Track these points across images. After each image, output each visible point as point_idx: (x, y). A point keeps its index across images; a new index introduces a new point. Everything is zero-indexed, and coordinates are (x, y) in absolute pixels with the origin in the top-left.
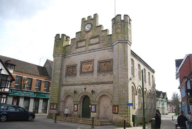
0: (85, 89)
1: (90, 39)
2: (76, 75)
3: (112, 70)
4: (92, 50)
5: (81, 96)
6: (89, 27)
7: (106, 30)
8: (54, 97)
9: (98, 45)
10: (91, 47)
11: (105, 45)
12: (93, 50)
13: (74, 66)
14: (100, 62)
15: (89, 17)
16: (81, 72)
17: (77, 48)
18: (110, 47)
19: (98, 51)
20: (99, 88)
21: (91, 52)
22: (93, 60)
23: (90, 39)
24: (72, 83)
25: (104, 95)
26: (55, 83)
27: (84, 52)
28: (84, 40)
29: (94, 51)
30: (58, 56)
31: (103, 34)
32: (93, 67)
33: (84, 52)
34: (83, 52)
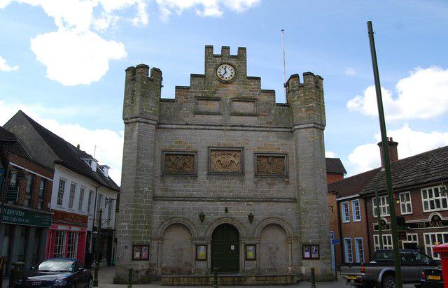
0: (226, 210)
1: (234, 100)
2: (195, 176)
3: (287, 177)
4: (241, 126)
5: (215, 225)
6: (222, 72)
7: (273, 92)
8: (141, 227)
9: (255, 118)
10: (236, 120)
11: (271, 123)
12: (243, 126)
13: (191, 155)
14: (260, 157)
15: (225, 49)
16: (211, 173)
19: (255, 131)
22: (243, 148)
23: (234, 100)
24: (184, 194)
25: (276, 224)
26: (142, 192)
28: (218, 99)
29: (244, 128)
30: (145, 123)
31: (265, 98)
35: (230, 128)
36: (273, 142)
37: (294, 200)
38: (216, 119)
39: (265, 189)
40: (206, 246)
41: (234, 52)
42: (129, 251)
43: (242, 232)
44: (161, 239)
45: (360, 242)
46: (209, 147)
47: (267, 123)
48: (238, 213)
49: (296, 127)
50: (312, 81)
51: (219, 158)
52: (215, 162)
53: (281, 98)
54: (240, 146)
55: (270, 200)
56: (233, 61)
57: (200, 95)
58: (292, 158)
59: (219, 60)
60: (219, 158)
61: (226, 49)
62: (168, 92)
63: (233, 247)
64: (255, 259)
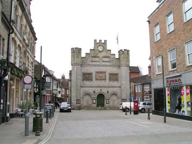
0: (101, 90)
1: (103, 57)
2: (92, 80)
5: (98, 94)
7: (114, 55)
8: (78, 95)
9: (109, 63)
10: (104, 63)
13: (91, 74)
14: (110, 74)
15: (100, 41)
16: (96, 79)
20: (111, 90)
23: (103, 57)
24: (89, 85)
25: (115, 94)
27: (99, 66)
28: (98, 57)
31: (112, 56)
32: (105, 76)
36: (114, 70)
37: (120, 87)
38: (98, 63)
40: (95, 100)
41: (103, 42)
42: (75, 101)
43: (105, 96)
44: (83, 98)
45: (140, 98)
48: (104, 91)
53: (117, 56)
55: (113, 87)
56: (103, 45)
57: (93, 56)
58: (120, 75)
59: (98, 45)
62: (83, 55)
64: (109, 103)
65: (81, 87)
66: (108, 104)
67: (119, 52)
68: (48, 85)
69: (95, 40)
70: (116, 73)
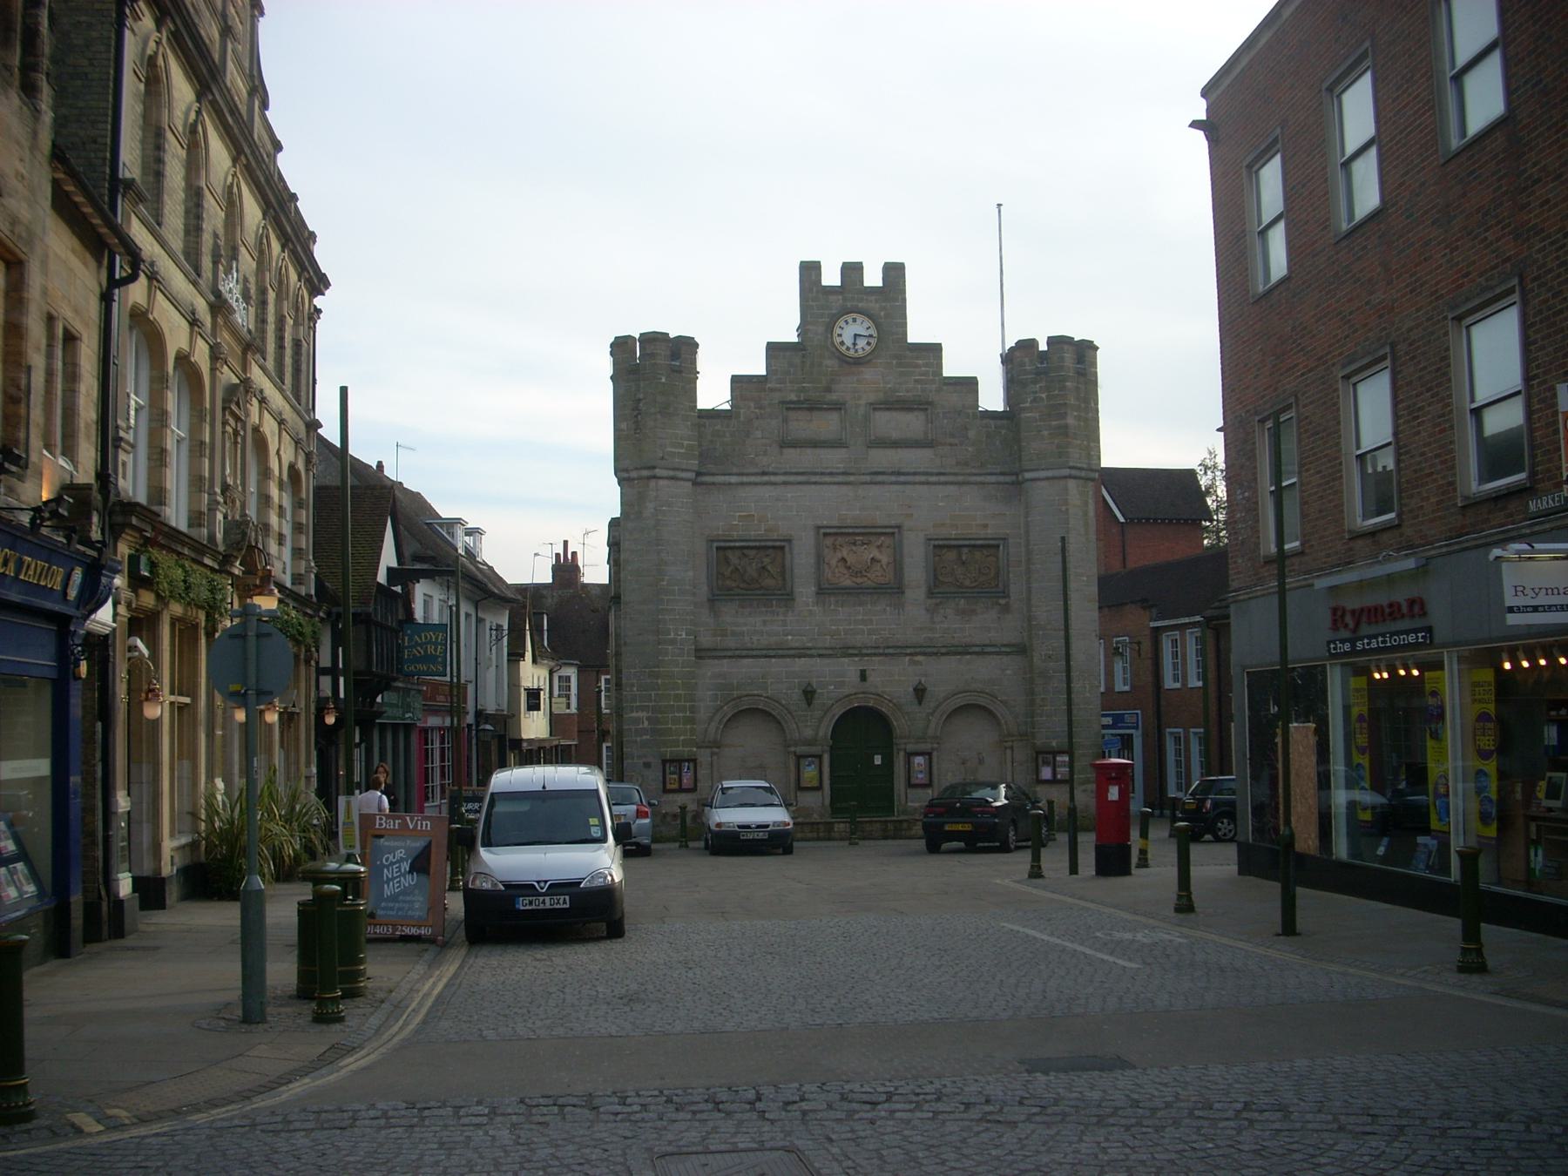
0: (863, 676)
1: (876, 407)
4: (893, 473)
5: (838, 711)
7: (970, 385)
9: (926, 454)
10: (883, 458)
11: (966, 464)
12: (899, 474)
13: (778, 549)
14: (939, 547)
17: (785, 444)
18: (993, 479)
19: (928, 483)
20: (945, 676)
21: (883, 483)
22: (899, 527)
26: (673, 642)
28: (838, 407)
29: (902, 478)
30: (672, 478)
32: (898, 565)
33: (840, 479)
34: (831, 474)
35: (868, 478)
37: (1022, 650)
38: (833, 459)
39: (953, 625)
43: (899, 724)
44: (716, 745)
46: (819, 528)
47: (958, 463)
49: (1028, 475)
50: (1069, 357)
51: (845, 553)
52: (834, 562)
53: (992, 398)
54: (893, 523)
55: (963, 650)
56: (873, 305)
57: (793, 397)
59: (836, 301)
60: (845, 553)
61: (852, 271)
62: (713, 393)
63: (878, 760)
65: (701, 653)
66: (920, 791)
67: (1008, 359)
68: (430, 649)
69: (810, 270)
70: (990, 532)
